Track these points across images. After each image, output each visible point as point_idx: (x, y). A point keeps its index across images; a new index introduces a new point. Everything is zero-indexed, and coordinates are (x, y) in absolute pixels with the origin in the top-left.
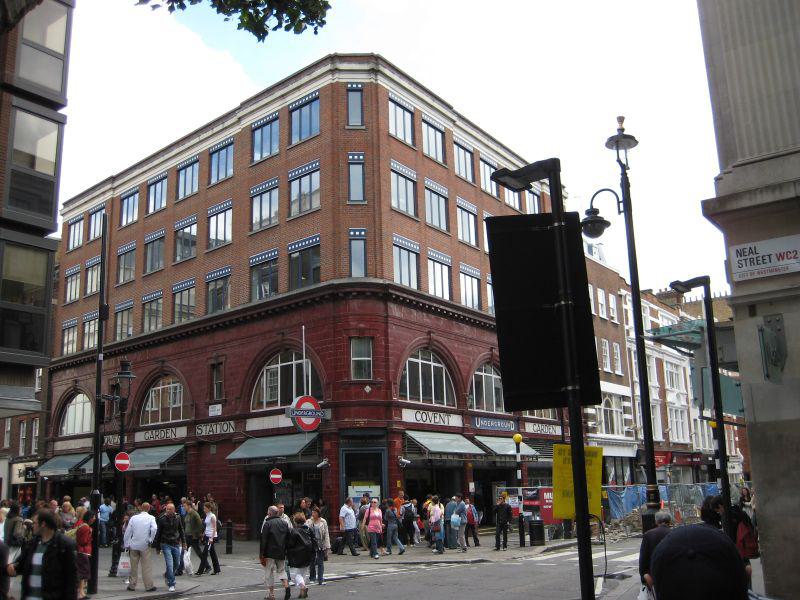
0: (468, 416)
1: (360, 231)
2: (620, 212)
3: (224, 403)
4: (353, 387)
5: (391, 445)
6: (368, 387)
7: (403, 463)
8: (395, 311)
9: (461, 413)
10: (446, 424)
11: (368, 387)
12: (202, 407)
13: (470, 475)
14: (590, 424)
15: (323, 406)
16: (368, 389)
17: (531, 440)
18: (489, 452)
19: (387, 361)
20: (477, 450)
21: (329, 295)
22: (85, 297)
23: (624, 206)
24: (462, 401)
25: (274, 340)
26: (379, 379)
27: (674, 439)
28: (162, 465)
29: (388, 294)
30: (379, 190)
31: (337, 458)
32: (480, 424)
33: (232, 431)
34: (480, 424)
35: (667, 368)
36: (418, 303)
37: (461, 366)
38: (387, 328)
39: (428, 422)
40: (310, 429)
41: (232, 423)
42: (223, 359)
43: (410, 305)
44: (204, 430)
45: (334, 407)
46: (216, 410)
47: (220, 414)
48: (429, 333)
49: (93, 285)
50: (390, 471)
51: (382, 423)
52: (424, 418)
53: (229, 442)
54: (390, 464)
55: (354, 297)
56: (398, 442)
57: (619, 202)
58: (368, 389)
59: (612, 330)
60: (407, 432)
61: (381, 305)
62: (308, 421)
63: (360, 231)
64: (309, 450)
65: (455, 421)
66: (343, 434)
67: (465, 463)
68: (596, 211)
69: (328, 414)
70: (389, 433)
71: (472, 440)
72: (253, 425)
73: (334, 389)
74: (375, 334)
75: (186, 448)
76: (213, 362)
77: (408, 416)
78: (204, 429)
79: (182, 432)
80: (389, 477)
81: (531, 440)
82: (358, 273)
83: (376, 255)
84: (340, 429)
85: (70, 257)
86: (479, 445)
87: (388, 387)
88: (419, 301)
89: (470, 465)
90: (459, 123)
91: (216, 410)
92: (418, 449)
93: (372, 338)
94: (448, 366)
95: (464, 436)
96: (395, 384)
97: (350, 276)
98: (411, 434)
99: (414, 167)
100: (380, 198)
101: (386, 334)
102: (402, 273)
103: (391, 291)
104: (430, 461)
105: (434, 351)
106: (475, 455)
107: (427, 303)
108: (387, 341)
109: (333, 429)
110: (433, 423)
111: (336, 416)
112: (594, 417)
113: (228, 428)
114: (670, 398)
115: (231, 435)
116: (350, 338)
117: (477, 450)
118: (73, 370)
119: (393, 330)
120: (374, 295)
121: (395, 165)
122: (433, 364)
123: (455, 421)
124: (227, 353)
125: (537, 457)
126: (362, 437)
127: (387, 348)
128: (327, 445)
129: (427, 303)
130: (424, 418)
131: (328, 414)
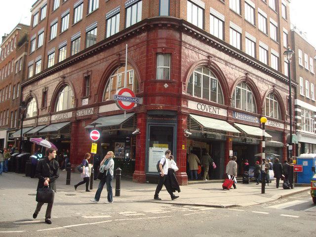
3: (90, 97)
4: (158, 84)
5: (179, 122)
6: (166, 84)
7: (187, 135)
8: (186, 38)
9: (227, 109)
10: (217, 114)
11: (166, 84)
12: (80, 100)
13: (230, 145)
15: (138, 96)
16: (166, 86)
18: (243, 134)
19: (180, 69)
20: (237, 131)
22: (38, 49)
24: (227, 101)
25: (114, 59)
26: (174, 80)
29: (181, 26)
31: (145, 129)
32: (238, 116)
33: (92, 113)
34: (238, 116)
36: (202, 36)
37: (228, 80)
39: (205, 111)
40: (129, 110)
41: (93, 109)
42: (90, 73)
43: (196, 37)
44: (80, 113)
46: (86, 102)
47: (87, 104)
49: (41, 43)
50: (178, 139)
51: (175, 108)
52: (203, 109)
53: (89, 119)
54: (178, 134)
55: (161, 28)
56: (184, 120)
58: (166, 86)
60: (190, 115)
61: (177, 35)
62: (127, 104)
64: (128, 123)
65: (223, 112)
66: (150, 113)
67: (228, 138)
69: (141, 101)
70: (179, 114)
71: (233, 125)
72: (103, 109)
73: (145, 85)
74: (174, 52)
75: (71, 123)
76: (85, 75)
77: (192, 105)
78: (80, 113)
79: (70, 115)
80: (178, 142)
87: (180, 85)
88: (203, 36)
89: (231, 140)
91: (86, 102)
92: (198, 126)
95: (228, 122)
96: (184, 84)
98: (193, 116)
101: (180, 53)
103: (184, 25)
104: (206, 134)
107: (208, 37)
108: (180, 57)
109: (142, 110)
110: (208, 112)
111: (145, 102)
115: (91, 115)
116: (157, 54)
117: (237, 131)
118: (30, 86)
119: (185, 51)
120: (173, 27)
122: (210, 77)
124: (92, 69)
125: (269, 139)
126: (162, 116)
128: (140, 120)
129: (208, 37)
130: (203, 109)
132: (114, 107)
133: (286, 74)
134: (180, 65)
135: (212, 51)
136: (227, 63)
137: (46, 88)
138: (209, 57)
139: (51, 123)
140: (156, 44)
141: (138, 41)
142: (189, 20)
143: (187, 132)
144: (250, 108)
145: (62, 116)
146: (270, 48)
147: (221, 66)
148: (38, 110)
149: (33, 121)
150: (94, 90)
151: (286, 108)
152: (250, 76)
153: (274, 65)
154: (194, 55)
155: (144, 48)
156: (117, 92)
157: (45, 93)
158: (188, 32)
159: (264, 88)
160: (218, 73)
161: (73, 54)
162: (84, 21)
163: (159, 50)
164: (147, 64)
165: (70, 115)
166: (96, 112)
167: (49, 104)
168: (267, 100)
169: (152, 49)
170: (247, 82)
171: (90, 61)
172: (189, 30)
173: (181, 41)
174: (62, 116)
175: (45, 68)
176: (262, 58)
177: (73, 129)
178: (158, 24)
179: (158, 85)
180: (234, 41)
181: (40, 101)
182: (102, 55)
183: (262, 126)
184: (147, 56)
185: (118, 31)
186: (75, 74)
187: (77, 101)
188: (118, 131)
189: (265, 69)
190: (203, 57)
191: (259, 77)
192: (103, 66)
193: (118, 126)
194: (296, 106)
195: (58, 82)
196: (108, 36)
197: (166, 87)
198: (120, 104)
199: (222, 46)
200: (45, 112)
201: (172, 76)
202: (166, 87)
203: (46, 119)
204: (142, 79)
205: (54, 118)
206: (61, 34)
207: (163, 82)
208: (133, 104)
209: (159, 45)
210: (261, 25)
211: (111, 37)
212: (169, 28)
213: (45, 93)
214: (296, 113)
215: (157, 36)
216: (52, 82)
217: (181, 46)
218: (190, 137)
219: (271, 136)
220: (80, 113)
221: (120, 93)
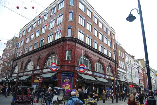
0: (93, 71)
1: (71, 27)
2: (138, 14)
3: (40, 66)
4: (66, 61)
8: (77, 45)
9: (92, 71)
13: (94, 86)
14: (119, 77)
15: (58, 66)
16: (69, 62)
17: (107, 79)
18: (98, 81)
20: (96, 80)
21: (62, 40)
22: (21, 46)
23: (140, 12)
27: (133, 82)
28: (26, 79)
29: (76, 40)
30: (76, 19)
31: (60, 79)
32: (96, 74)
35: (132, 69)
37: (93, 61)
38: (75, 48)
40: (54, 71)
43: (81, 44)
44: (35, 72)
45: (61, 66)
46: (38, 68)
48: (86, 52)
49: (22, 44)
53: (39, 74)
55: (68, 41)
57: (138, 11)
59: (123, 60)
61: (74, 43)
62: (54, 69)
63: (71, 27)
64: (54, 76)
65: (91, 73)
68: (132, 15)
69: (59, 68)
71: (95, 78)
72: (45, 71)
74: (72, 49)
76: (39, 57)
79: (31, 72)
80: (73, 84)
81: (107, 79)
82: (69, 35)
83: (74, 32)
84: (62, 71)
85: (20, 39)
86: (96, 79)
87: (74, 62)
88: (83, 44)
89: (94, 83)
90: (95, 12)
91: (38, 68)
92: (81, 78)
93: (71, 50)
94: (89, 60)
97: (68, 36)
99: (85, 17)
100: (76, 20)
102: (80, 37)
103: (77, 40)
104: (84, 81)
105: (87, 56)
106: (94, 81)
108: (75, 52)
109: (59, 71)
111: (61, 68)
112: (119, 76)
113: (39, 72)
114: (133, 74)
116: (66, 50)
117: (96, 80)
119: (77, 49)
120: (72, 41)
121: (80, 14)
122: (86, 59)
123: (91, 73)
125: (108, 83)
127: (75, 53)
131: (59, 68)
132: (48, 70)
133: (114, 59)
134: (75, 55)
135: (87, 50)
136: (92, 54)
137: (23, 62)
138: (86, 52)
139: (24, 76)
140: (66, 46)
141: (59, 45)
142: (79, 38)
143: (77, 80)
144: (102, 71)
145: (28, 73)
146: (108, 49)
147: (90, 55)
148: (19, 70)
149: (16, 75)
150: (42, 63)
151: (114, 71)
152: (101, 59)
153: (110, 55)
154: (80, 51)
155: (61, 48)
156: (51, 64)
157: (22, 64)
158: (78, 43)
159: (106, 64)
160: (88, 58)
161: (34, 49)
162: (39, 37)
163: (67, 49)
164: (62, 54)
165: (31, 72)
166: (42, 72)
167: (23, 68)
168: (107, 68)
169: (65, 48)
170: (100, 61)
171: (40, 52)
172: (78, 42)
173: (75, 46)
174: (28, 73)
175: (23, 54)
176: (105, 53)
177: (32, 78)
178: (67, 39)
179: (66, 62)
180: (95, 46)
181: (20, 67)
182: (45, 50)
183: (105, 78)
184: (62, 51)
185: (52, 41)
186: (35, 57)
187: (34, 67)
188: (50, 80)
189: (107, 57)
190: (83, 52)
191: (104, 60)
192: (45, 54)
193: (50, 78)
194: (118, 71)
195: (28, 60)
196: (48, 43)
197: (69, 63)
198: (51, 69)
199: (91, 48)
200: (22, 71)
201: (72, 59)
202: (69, 63)
203: (22, 74)
204: (60, 59)
205: (25, 74)
206: (30, 41)
207: (68, 61)
208: (56, 69)
209: (67, 47)
210: (105, 41)
211: (49, 43)
212: (71, 41)
213: (22, 64)
214: (118, 73)
215: (67, 44)
216: (25, 60)
217: (75, 47)
218: (78, 82)
219: (109, 82)
220: (35, 72)
221: (51, 65)
